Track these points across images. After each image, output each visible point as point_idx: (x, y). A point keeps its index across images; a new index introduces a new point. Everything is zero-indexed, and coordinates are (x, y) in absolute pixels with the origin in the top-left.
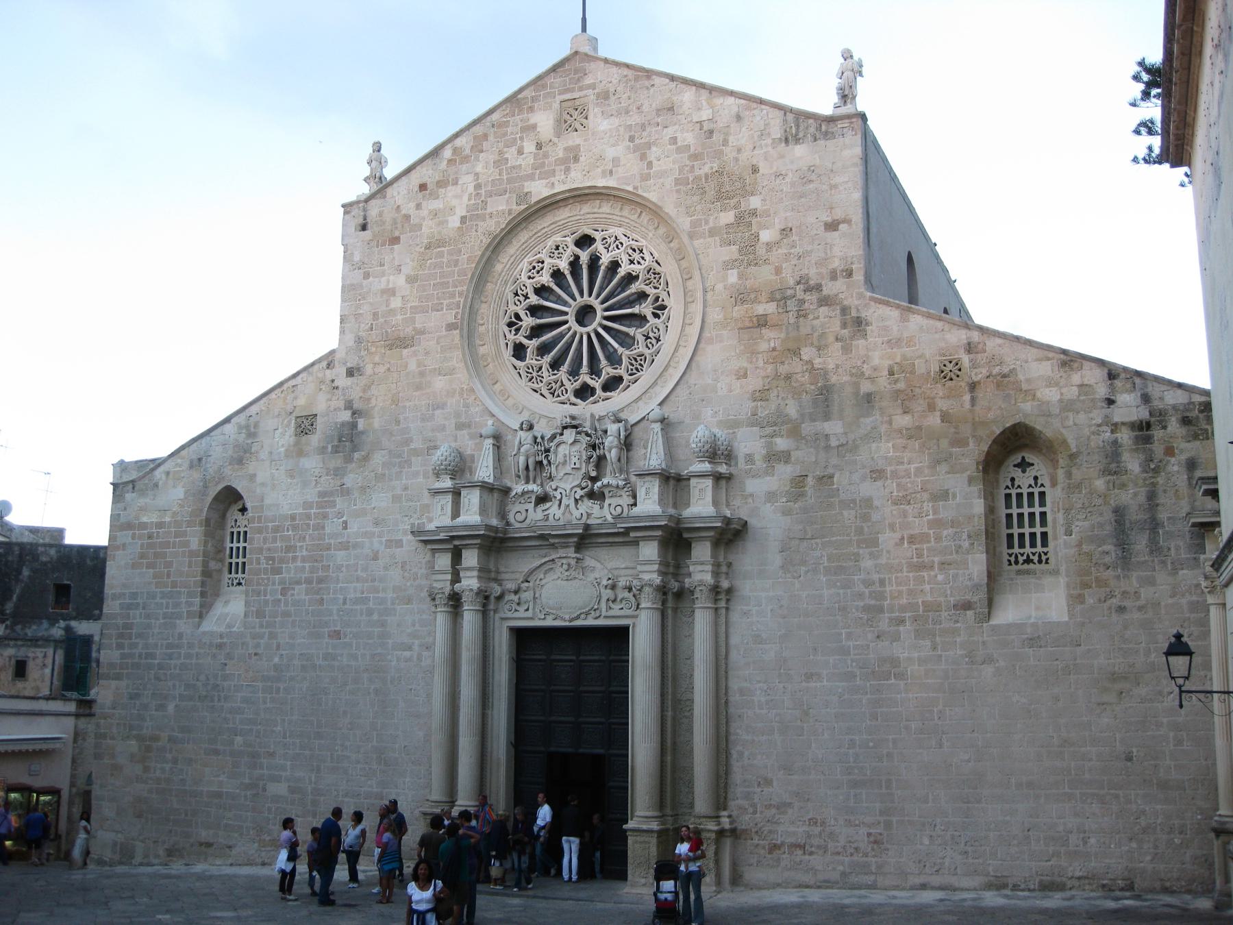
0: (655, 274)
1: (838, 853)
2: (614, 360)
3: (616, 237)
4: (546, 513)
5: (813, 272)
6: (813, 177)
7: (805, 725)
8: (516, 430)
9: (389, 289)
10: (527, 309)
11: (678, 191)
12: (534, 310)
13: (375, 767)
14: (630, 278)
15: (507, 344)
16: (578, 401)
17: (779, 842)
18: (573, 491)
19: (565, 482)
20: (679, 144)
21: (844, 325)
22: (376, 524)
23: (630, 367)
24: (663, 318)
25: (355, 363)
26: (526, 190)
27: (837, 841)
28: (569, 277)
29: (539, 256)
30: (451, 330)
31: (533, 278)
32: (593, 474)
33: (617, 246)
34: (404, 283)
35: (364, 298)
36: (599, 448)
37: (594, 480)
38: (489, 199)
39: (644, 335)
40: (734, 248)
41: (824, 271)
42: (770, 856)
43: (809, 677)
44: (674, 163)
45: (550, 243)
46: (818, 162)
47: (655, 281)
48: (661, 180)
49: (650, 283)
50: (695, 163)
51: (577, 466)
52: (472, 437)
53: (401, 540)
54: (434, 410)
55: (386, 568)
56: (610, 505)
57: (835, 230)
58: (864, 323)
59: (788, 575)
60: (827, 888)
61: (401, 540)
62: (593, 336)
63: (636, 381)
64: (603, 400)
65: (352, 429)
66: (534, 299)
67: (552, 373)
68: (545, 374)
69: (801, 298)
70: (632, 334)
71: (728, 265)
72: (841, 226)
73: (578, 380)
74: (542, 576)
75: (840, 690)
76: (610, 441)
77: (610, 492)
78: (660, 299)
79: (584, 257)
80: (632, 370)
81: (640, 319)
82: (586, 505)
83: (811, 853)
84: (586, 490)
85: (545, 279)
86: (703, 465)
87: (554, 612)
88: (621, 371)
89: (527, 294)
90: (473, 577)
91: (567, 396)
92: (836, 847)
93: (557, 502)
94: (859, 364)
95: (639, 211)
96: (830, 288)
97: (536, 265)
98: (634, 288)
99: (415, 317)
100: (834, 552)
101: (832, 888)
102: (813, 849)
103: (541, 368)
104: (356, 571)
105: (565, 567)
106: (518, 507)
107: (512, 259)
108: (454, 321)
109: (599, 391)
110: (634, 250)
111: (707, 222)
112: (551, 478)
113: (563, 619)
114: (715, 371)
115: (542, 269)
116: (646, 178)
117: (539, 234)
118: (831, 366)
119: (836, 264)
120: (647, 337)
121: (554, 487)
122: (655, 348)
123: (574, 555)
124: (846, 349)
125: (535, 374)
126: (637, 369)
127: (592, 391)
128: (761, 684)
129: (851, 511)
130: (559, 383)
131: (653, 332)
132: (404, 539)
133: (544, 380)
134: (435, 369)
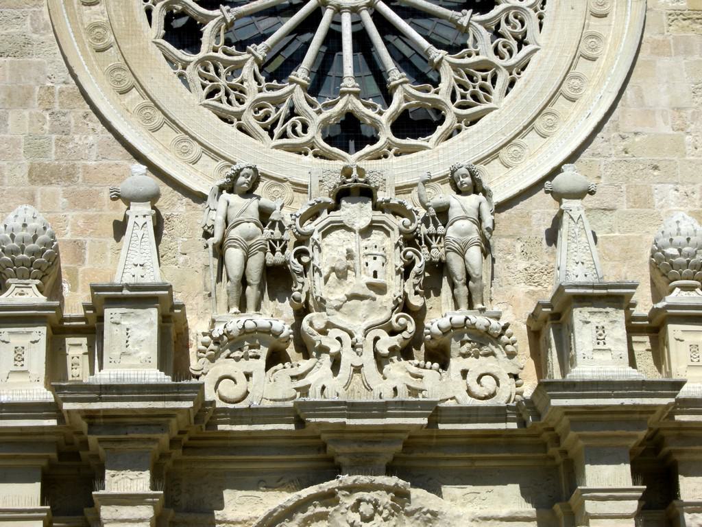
2: (423, 75)
4: (301, 383)
8: (200, 198)
15: (149, 12)
16: (336, 150)
19: (351, 313)
23: (459, 91)
32: (416, 301)
39: (488, 29)
51: (379, 280)
52: (79, 201)
56: (464, 373)
62: (346, 19)
63: (473, 122)
67: (264, 84)
68: (250, 85)
70: (464, 21)
73: (333, 104)
76: (460, 229)
77: (463, 344)
80: (463, 97)
82: (399, 371)
84: (405, 334)
86: (693, 294)
90: (141, 520)
93: (326, 360)
105: (366, 509)
106: (225, 366)
109: (386, 135)
114: (679, 109)
120: (497, 34)
121: (319, 324)
122: (517, 57)
123: (392, 481)
126: (474, 96)
130: (284, 109)
131: (507, 21)
133: (249, 100)
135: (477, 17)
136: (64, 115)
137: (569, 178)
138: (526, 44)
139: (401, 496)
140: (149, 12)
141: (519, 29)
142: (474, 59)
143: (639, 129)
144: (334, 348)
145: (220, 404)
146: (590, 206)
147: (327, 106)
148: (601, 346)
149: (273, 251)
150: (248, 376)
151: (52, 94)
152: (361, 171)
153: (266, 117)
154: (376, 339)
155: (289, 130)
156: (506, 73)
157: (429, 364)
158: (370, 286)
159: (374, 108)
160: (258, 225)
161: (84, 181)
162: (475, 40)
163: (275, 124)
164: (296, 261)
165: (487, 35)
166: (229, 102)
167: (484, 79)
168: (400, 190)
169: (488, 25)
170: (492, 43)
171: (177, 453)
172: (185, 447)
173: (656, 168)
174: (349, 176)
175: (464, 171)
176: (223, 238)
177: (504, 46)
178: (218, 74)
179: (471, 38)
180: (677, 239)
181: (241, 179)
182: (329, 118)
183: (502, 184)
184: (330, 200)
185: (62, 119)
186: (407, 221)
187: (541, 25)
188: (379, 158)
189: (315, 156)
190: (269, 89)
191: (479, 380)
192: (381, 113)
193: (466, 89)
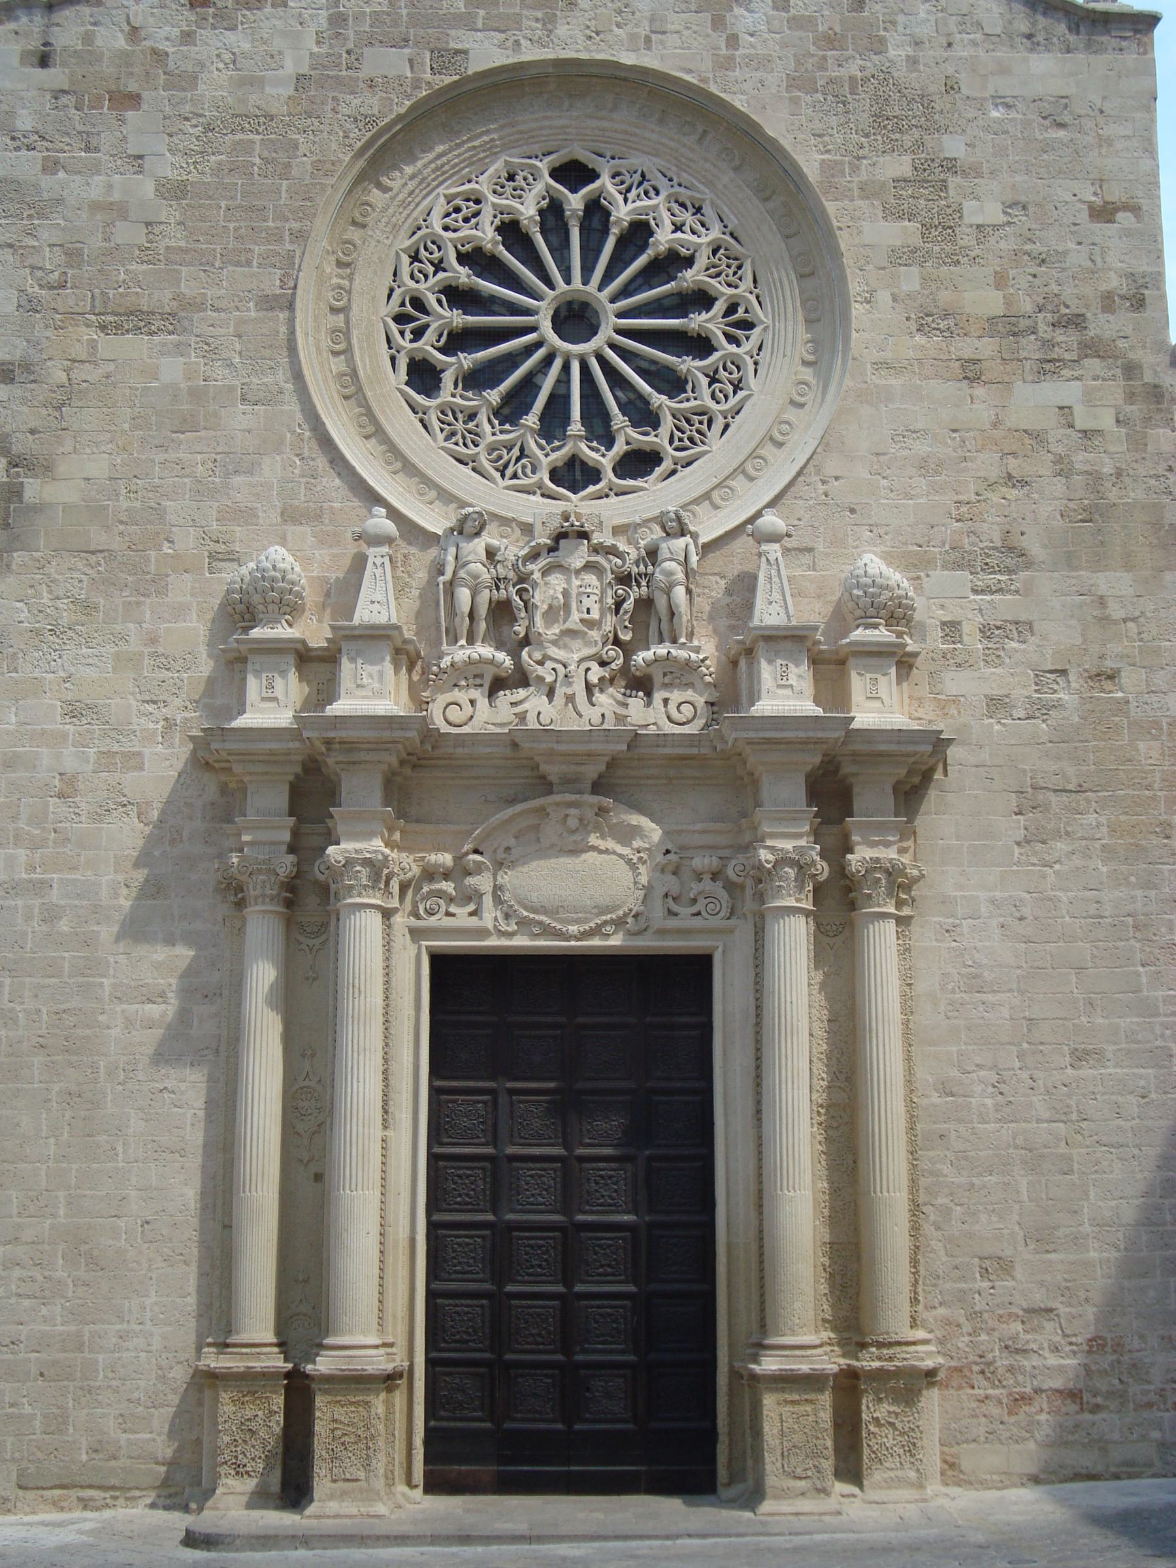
0: (728, 258)
1: (1149, 1405)
2: (646, 417)
3: (643, 175)
4: (518, 709)
5: (1068, 293)
6: (1066, 118)
7: (1074, 1152)
9: (111, 203)
10: (440, 292)
11: (795, 101)
12: (455, 296)
13: (63, 1274)
14: (674, 261)
17: (1028, 1390)
18: (585, 665)
19: (565, 647)
20: (793, 11)
21: (1130, 397)
22: (74, 712)
24: (747, 346)
25: (18, 353)
26: (453, 45)
27: (1149, 1382)
28: (539, 240)
29: (467, 186)
30: (272, 309)
31: (455, 231)
32: (626, 637)
33: (646, 193)
34: (152, 196)
35: (42, 216)
36: (639, 586)
37: (627, 649)
38: (366, 50)
39: (707, 376)
40: (913, 226)
41: (1088, 291)
42: (1013, 1419)
43: (1079, 1057)
44: (784, 45)
45: (497, 167)
46: (1071, 90)
47: (731, 272)
48: (758, 74)
49: (718, 275)
50: (830, 53)
53: (139, 754)
54: (227, 475)
55: (97, 817)
57: (1109, 221)
58: (1167, 397)
59: (1034, 860)
60: (1130, 1476)
61: (139, 754)
63: (689, 464)
64: (616, 495)
65: (9, 501)
66: (463, 275)
67: (498, 427)
69: (1047, 337)
70: (684, 368)
71: (901, 257)
72: (1120, 216)
74: (512, 842)
75: (1142, 1083)
77: (665, 674)
78: (741, 310)
79: (575, 202)
80: (681, 440)
81: (701, 346)
82: (606, 700)
83: (1096, 1409)
85: (487, 235)
86: (877, 632)
87: (542, 918)
88: (659, 439)
89: (441, 261)
91: (534, 479)
92: (1145, 1393)
94: (1161, 471)
95: (700, 129)
96: (1102, 326)
97: (463, 204)
98: (691, 277)
99: (179, 272)
100: (1123, 818)
101: (1138, 1476)
102: (1099, 1400)
103: (472, 416)
104: (15, 818)
107: (411, 185)
108: (278, 292)
110: (683, 205)
111: (855, 169)
112: (526, 641)
113: (560, 935)
115: (476, 214)
116: (726, 64)
117: (476, 143)
118: (1107, 470)
119: (1113, 282)
120: (713, 380)
121: (538, 655)
122: (733, 401)
124: (1137, 442)
125: (459, 426)
126: (691, 440)
127: (593, 475)
128: (982, 1073)
129: (1152, 743)
130: (516, 452)
132: (147, 752)
134: (231, 389)
135: (698, 363)
136: (313, 460)
137: (772, 521)
138: (741, 389)
139: (602, 811)
140: (393, 359)
141: (735, 375)
142: (693, 403)
143: (838, 474)
144: (549, 679)
145: (445, 729)
146: (789, 546)
147: (553, 450)
148: (783, 682)
149: (498, 589)
150: (472, 702)
151: (302, 440)
152: (578, 516)
153: (500, 457)
154: (588, 669)
155: (520, 471)
156: (720, 417)
157: (634, 692)
158: (582, 620)
159: (597, 450)
160: (484, 566)
161: (330, 521)
162: (694, 387)
163: (506, 466)
164: (517, 599)
165: (704, 381)
166: (465, 445)
167: (701, 423)
168: (617, 531)
169: (706, 371)
170: (710, 386)
171: (407, 771)
172: (414, 767)
173: (852, 511)
174: (567, 520)
175: (673, 516)
176: (454, 573)
177: (721, 391)
178: (456, 419)
179: (690, 384)
180: (864, 580)
181: (469, 524)
182: (556, 459)
183: (709, 526)
184: (549, 542)
185: (312, 463)
186: (619, 562)
187: (756, 371)
188: (601, 498)
189: (543, 495)
190: (501, 432)
191: (678, 707)
192: (603, 456)
193: (683, 433)
